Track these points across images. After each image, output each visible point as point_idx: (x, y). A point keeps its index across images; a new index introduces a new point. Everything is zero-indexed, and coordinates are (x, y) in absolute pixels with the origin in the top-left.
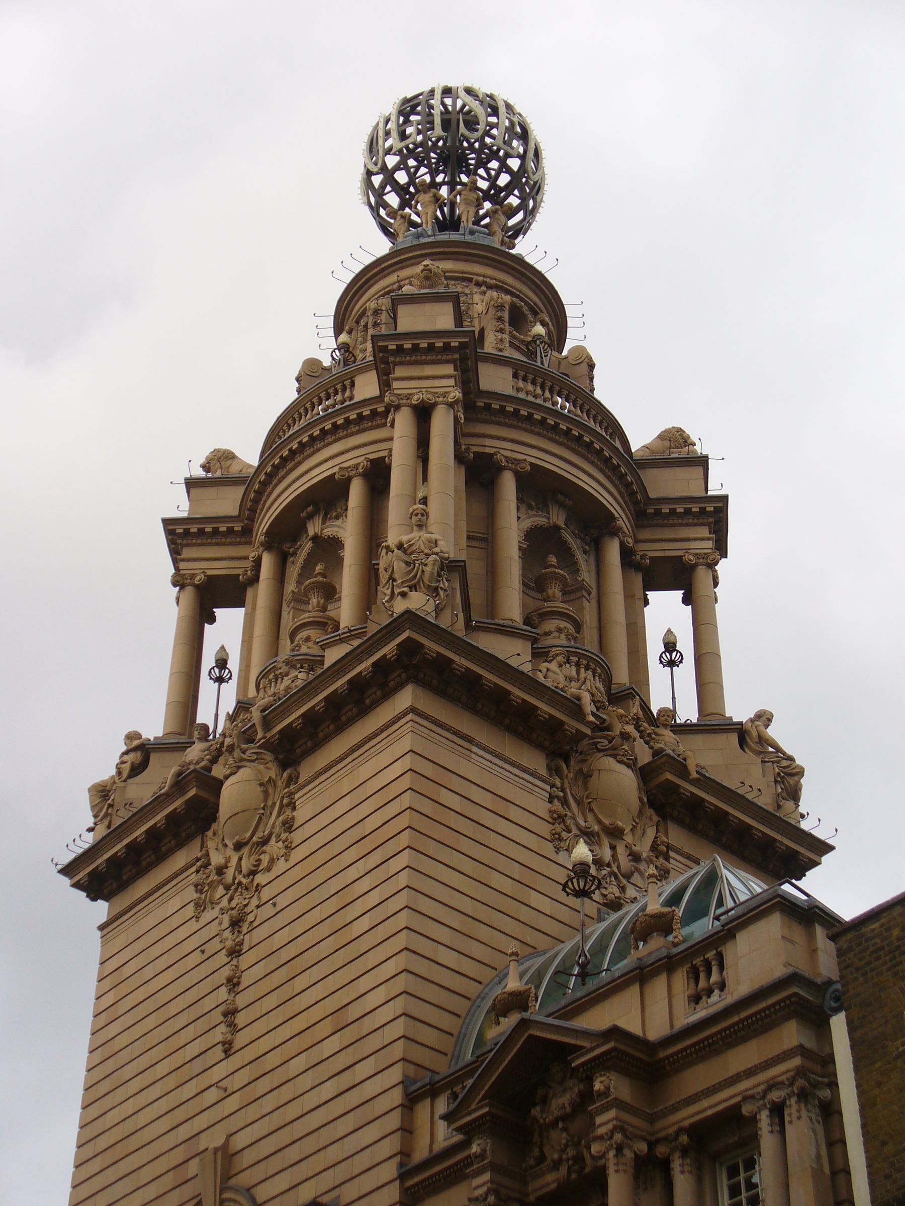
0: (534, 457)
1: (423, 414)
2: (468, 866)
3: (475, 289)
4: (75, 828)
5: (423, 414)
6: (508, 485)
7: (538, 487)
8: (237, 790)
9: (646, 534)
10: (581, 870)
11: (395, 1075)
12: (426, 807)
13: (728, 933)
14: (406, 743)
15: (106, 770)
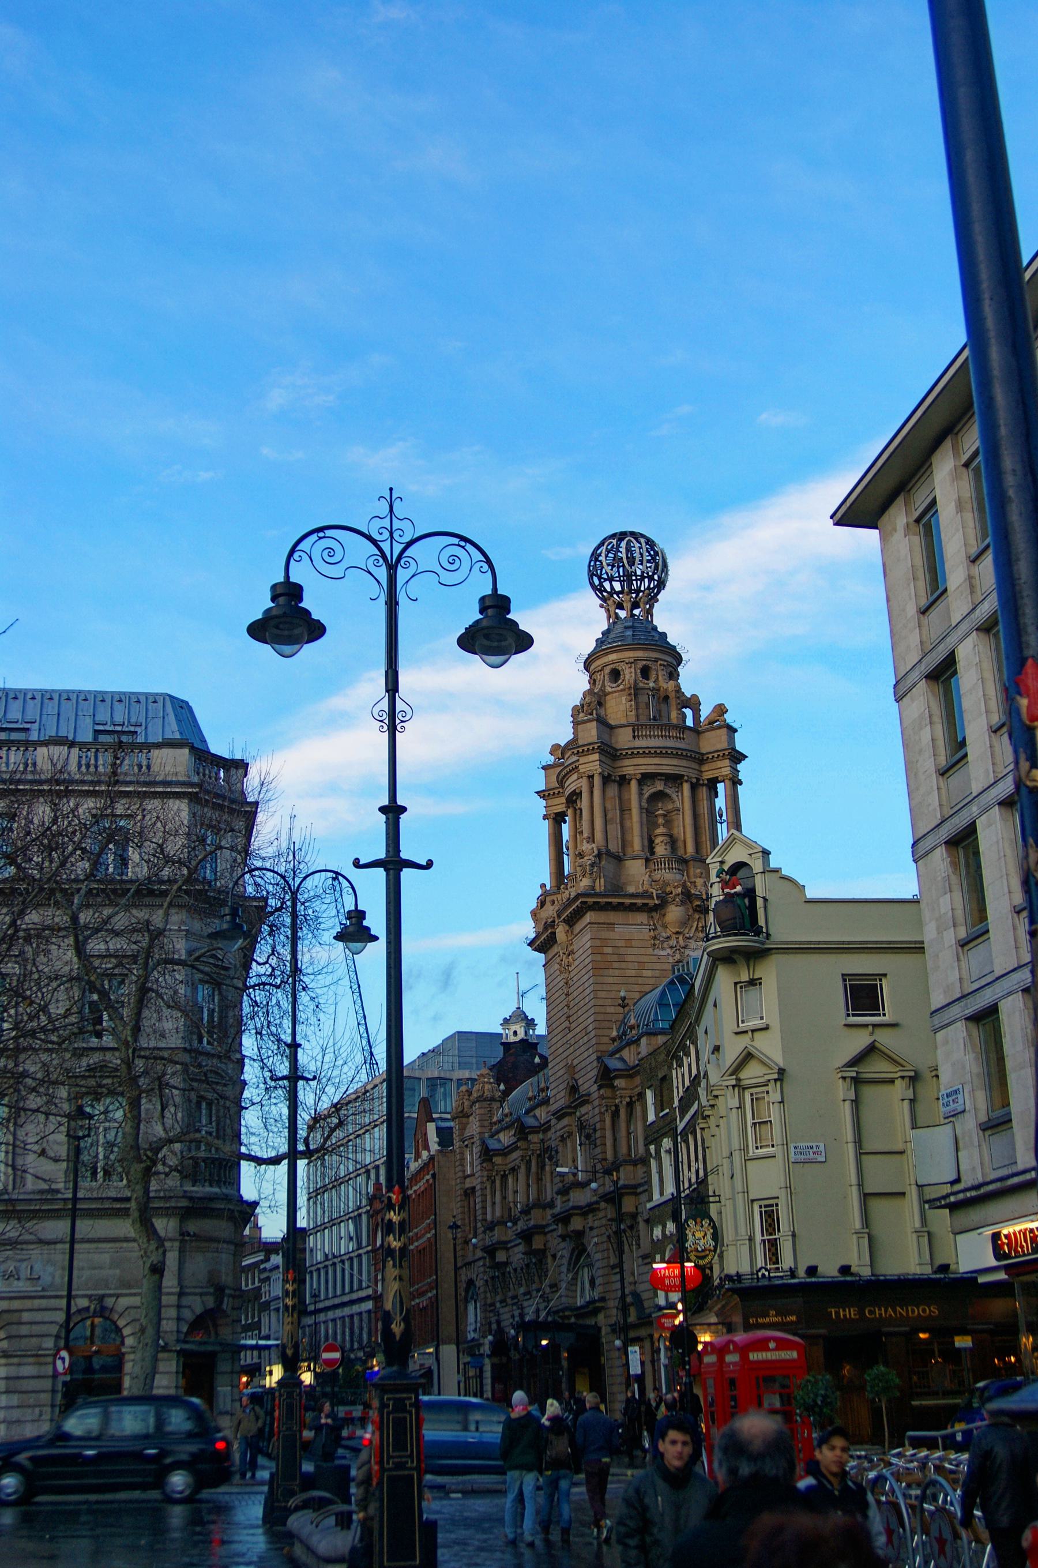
0: (643, 770)
1: (591, 777)
2: (617, 973)
3: (627, 666)
4: (528, 929)
5: (591, 777)
6: (634, 784)
7: (646, 778)
8: (561, 932)
9: (705, 768)
10: (624, 999)
11: (594, 1057)
12: (598, 958)
13: (639, 1039)
14: (588, 936)
15: (533, 904)
